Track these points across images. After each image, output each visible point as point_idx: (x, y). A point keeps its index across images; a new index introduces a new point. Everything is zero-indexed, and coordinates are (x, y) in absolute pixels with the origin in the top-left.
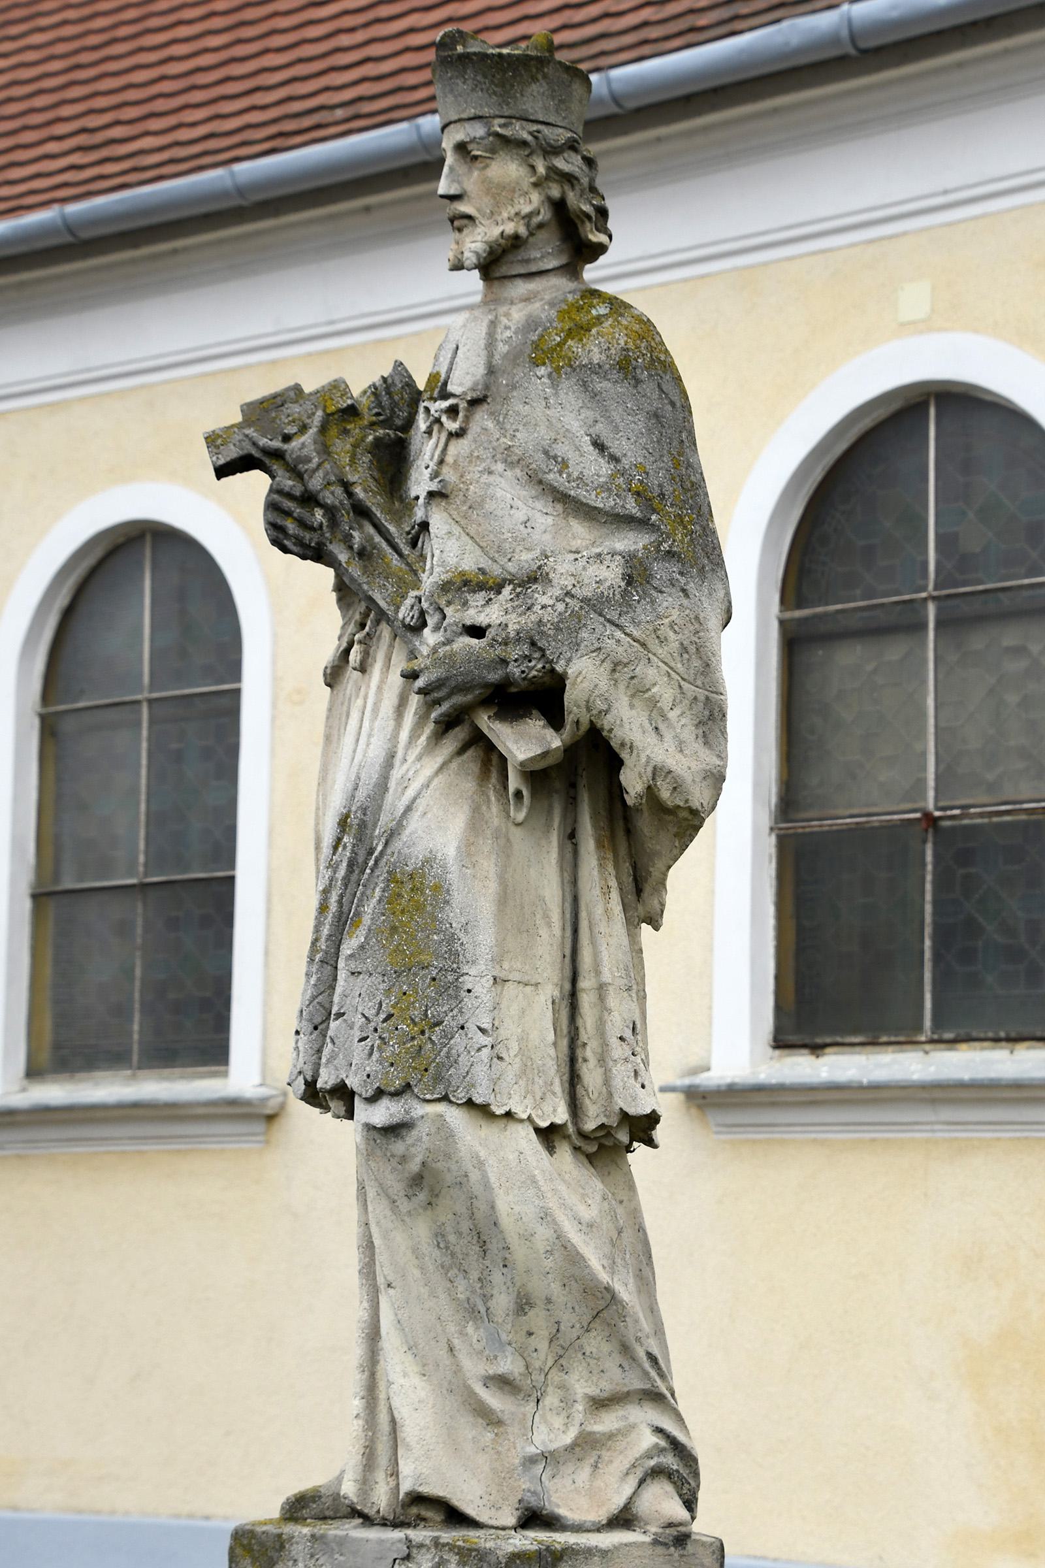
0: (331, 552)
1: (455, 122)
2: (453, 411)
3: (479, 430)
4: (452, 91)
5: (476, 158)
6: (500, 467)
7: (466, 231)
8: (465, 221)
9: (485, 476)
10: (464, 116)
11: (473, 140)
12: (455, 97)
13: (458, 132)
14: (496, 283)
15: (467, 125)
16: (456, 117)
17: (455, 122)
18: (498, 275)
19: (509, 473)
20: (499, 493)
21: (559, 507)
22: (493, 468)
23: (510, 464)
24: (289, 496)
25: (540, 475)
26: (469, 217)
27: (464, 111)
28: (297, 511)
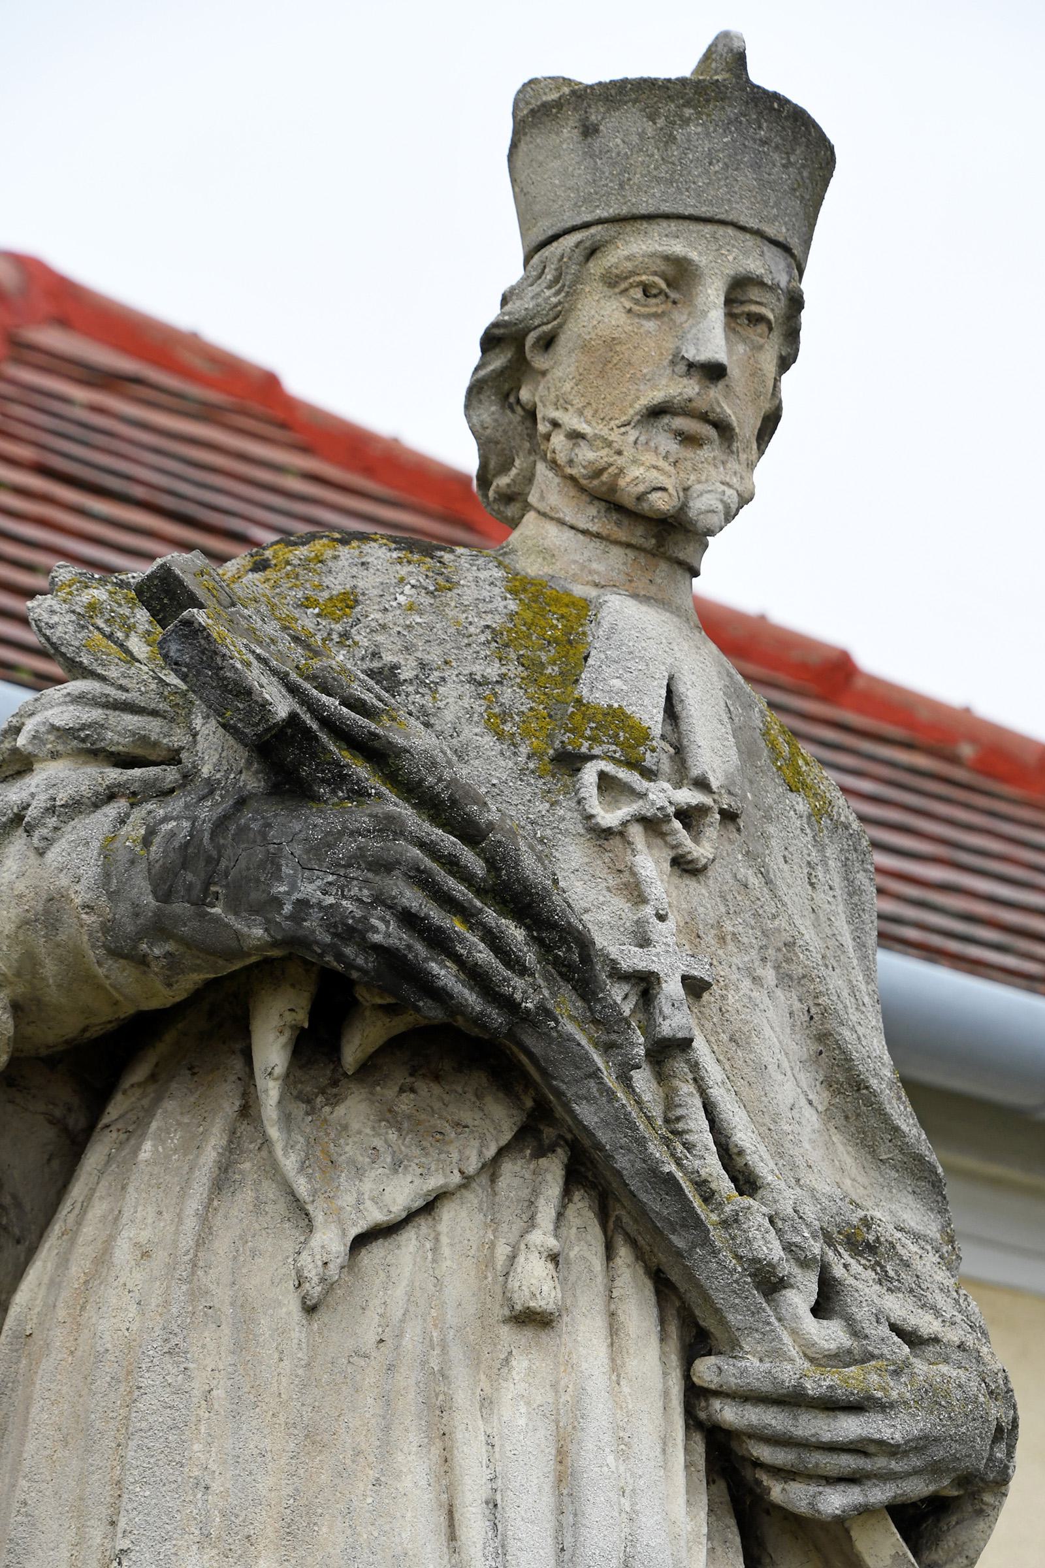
0: (570, 1038)
1: (743, 229)
2: (689, 816)
3: (728, 876)
4: (756, 166)
5: (756, 319)
6: (769, 975)
7: (705, 453)
8: (712, 433)
9: (747, 983)
10: (770, 231)
11: (773, 288)
12: (763, 184)
13: (746, 254)
14: (663, 566)
15: (771, 252)
16: (753, 223)
17: (743, 229)
18: (681, 556)
19: (779, 992)
20: (768, 1032)
21: (821, 1098)
22: (760, 972)
23: (786, 979)
24: (452, 864)
25: (832, 1024)
26: (724, 429)
27: (772, 220)
28: (490, 915)
